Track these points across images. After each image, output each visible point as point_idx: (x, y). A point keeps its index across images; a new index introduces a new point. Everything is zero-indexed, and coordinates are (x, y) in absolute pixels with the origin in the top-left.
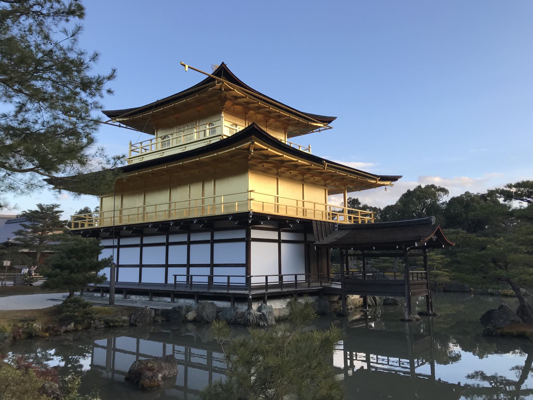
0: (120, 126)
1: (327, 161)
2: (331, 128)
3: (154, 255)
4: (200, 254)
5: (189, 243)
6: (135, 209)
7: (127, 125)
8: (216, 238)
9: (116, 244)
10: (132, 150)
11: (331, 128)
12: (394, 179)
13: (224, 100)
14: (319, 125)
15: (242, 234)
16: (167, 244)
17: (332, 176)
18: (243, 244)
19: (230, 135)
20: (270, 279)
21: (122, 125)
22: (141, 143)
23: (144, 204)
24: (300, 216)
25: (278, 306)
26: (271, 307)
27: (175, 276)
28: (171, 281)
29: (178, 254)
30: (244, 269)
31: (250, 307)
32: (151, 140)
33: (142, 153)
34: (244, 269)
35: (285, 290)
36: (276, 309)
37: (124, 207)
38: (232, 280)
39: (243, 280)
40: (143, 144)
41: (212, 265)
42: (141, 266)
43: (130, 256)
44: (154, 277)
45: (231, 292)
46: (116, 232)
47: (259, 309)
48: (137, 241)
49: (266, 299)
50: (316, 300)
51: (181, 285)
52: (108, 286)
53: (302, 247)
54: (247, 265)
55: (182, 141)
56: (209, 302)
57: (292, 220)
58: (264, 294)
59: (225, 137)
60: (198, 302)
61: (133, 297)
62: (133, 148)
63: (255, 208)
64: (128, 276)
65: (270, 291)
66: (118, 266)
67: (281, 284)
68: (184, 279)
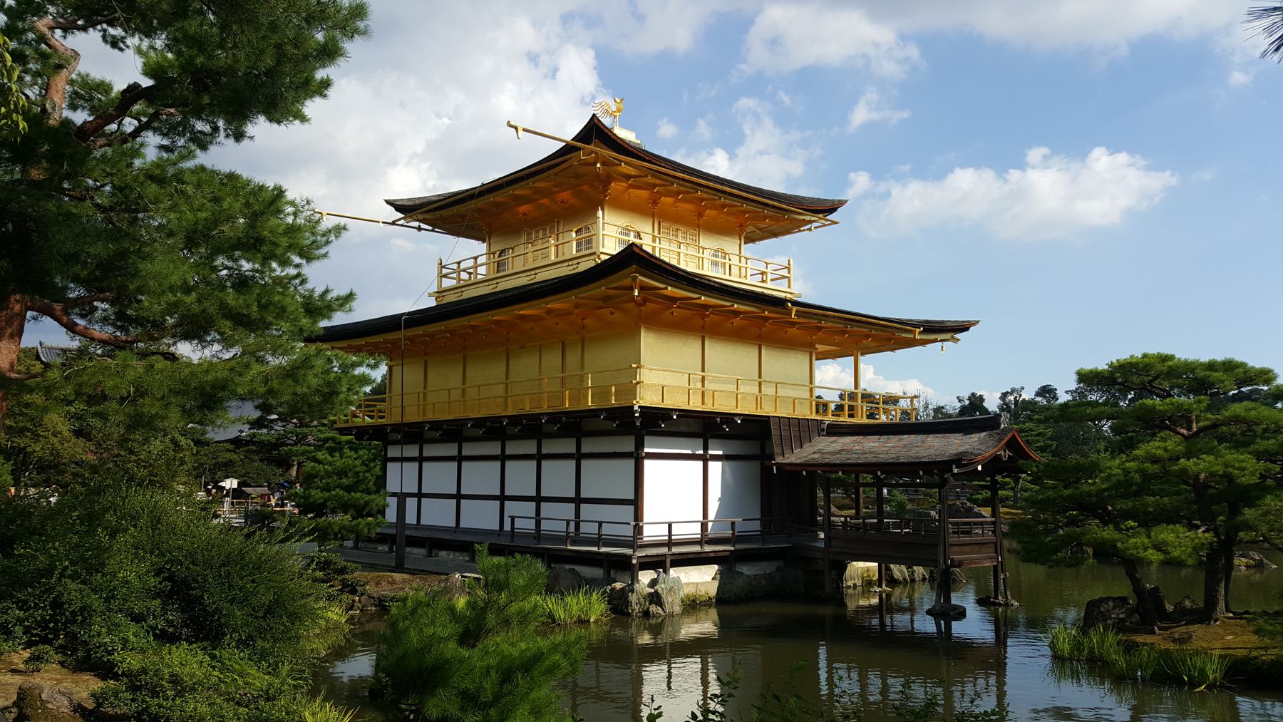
0: (419, 229)
1: (795, 303)
2: (835, 223)
3: (481, 477)
4: (558, 478)
5: (539, 457)
6: (447, 390)
7: (434, 226)
8: (585, 449)
9: (416, 454)
10: (445, 276)
11: (835, 223)
12: (962, 327)
13: (606, 181)
14: (808, 218)
15: (627, 445)
16: (503, 458)
17: (820, 328)
18: (632, 462)
19: (614, 253)
20: (676, 530)
21: (423, 226)
22: (459, 263)
23: (464, 383)
24: (748, 408)
25: (702, 579)
26: (678, 580)
27: (513, 519)
28: (507, 527)
29: (521, 477)
30: (630, 509)
31: (634, 579)
32: (476, 258)
33: (460, 280)
34: (630, 509)
35: (708, 548)
36: (688, 584)
37: (429, 388)
38: (607, 529)
39: (628, 531)
40: (463, 266)
41: (578, 500)
42: (459, 497)
43: (440, 477)
44: (481, 517)
45: (604, 549)
46: (414, 434)
47: (653, 583)
48: (451, 450)
49: (668, 564)
50: (778, 569)
51: (524, 535)
52: (393, 531)
53: (754, 467)
54: (636, 502)
55: (530, 260)
56: (568, 567)
57: (728, 418)
58: (664, 555)
59: (604, 257)
60: (549, 566)
61: (443, 554)
62: (445, 271)
63: (647, 398)
64: (438, 515)
65: (675, 550)
66: (420, 495)
67: (704, 540)
68: (531, 525)
